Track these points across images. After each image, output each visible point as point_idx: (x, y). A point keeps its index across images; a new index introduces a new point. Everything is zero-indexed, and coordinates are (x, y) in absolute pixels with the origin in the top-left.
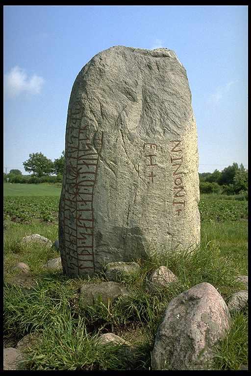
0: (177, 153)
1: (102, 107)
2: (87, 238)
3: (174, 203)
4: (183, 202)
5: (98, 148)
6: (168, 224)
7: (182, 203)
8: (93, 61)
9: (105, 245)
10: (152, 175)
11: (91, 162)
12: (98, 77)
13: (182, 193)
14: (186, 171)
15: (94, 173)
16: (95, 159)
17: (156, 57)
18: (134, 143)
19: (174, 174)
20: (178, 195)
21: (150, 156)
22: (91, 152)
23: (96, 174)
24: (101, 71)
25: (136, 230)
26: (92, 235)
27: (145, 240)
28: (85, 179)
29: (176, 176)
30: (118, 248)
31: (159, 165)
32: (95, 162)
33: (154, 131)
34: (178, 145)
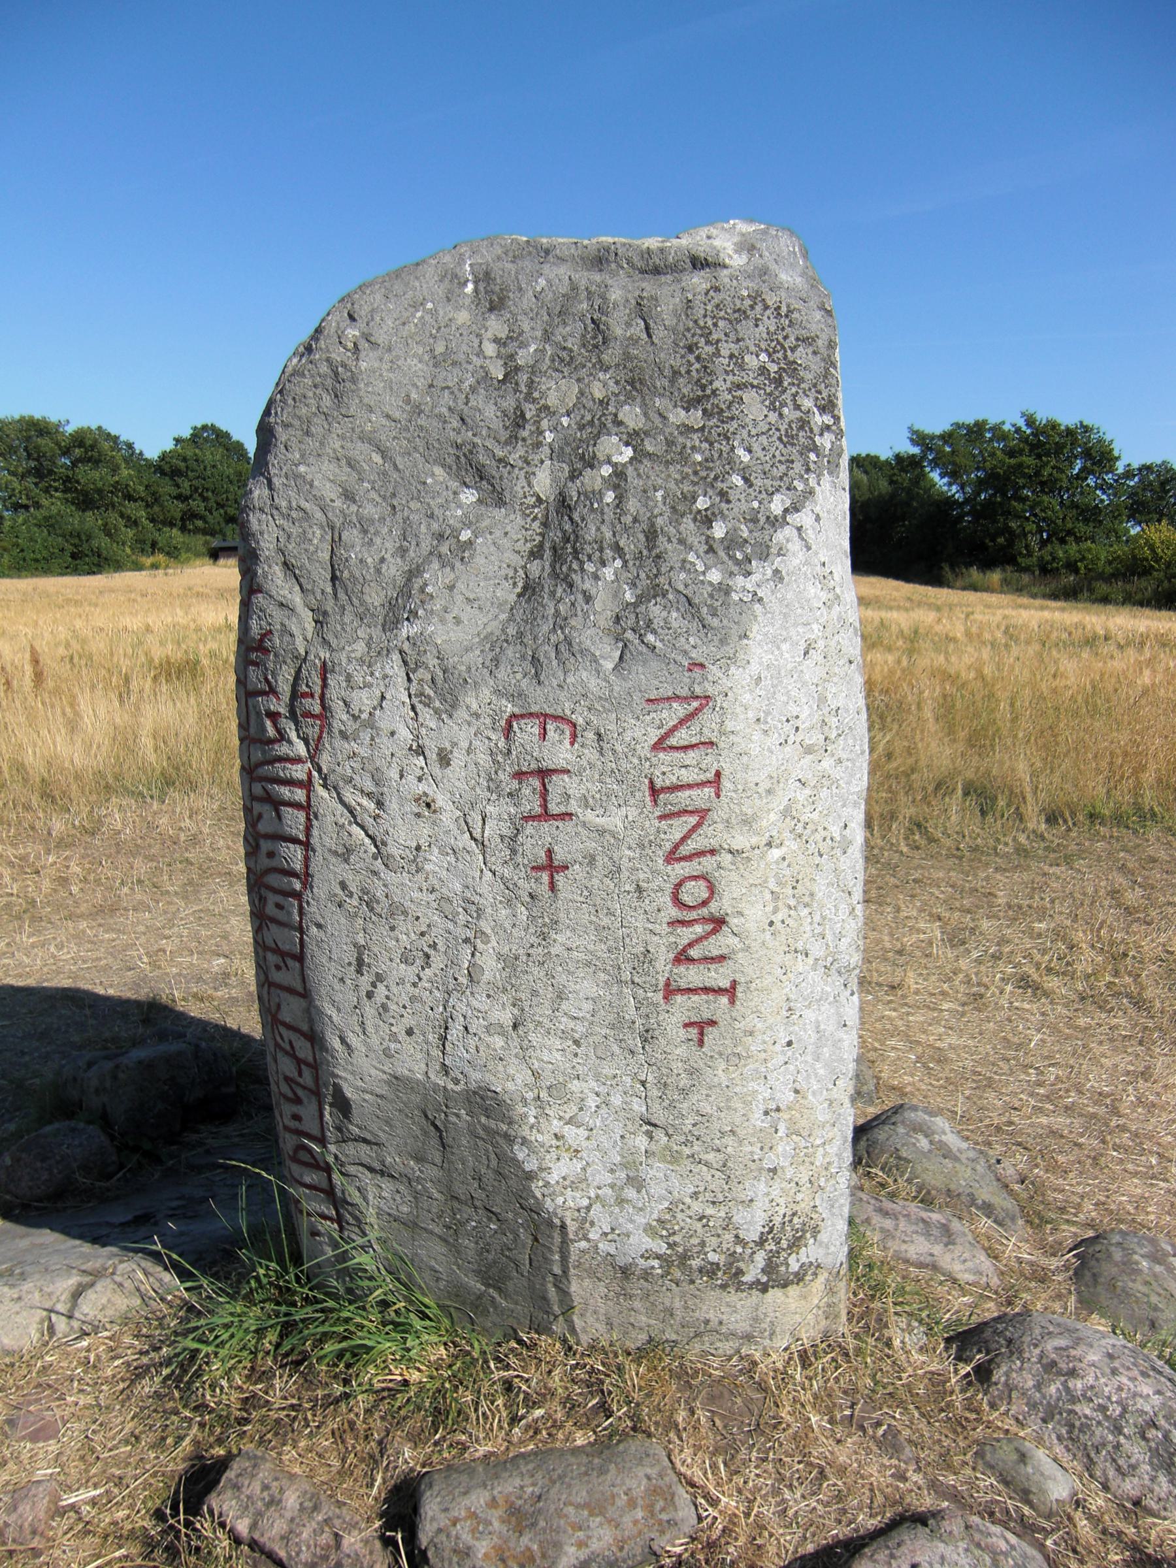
0: (691, 757)
2: (305, 1100)
3: (670, 991)
4: (725, 984)
5: (309, 731)
6: (643, 1083)
7: (719, 991)
8: (319, 331)
9: (365, 1141)
10: (551, 866)
11: (285, 792)
12: (327, 401)
13: (714, 946)
14: (740, 841)
15: (295, 841)
16: (299, 784)
17: (657, 271)
20: (694, 953)
21: (544, 774)
22: (283, 749)
23: (307, 845)
24: (336, 374)
25: (486, 1103)
26: (317, 1094)
28: (273, 863)
29: (681, 869)
30: (419, 1159)
31: (590, 816)
32: (300, 795)
33: (567, 650)
34: (698, 710)
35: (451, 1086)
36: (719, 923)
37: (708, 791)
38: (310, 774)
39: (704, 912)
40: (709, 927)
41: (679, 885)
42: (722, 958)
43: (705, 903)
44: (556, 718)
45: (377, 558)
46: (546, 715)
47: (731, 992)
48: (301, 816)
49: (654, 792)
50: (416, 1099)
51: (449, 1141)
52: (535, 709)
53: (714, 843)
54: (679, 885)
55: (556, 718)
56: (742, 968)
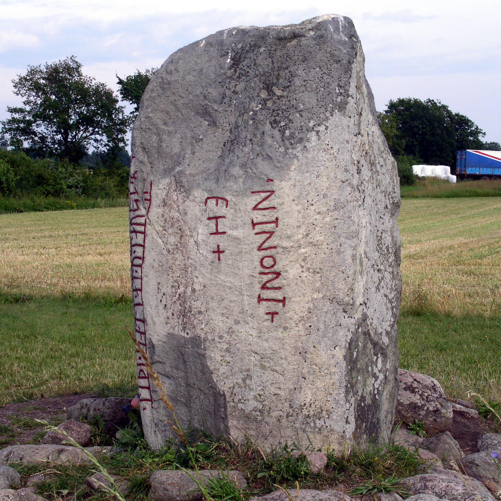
0: (266, 212)
1: (161, 140)
3: (260, 299)
4: (281, 298)
10: (218, 251)
12: (161, 91)
13: (276, 283)
14: (286, 243)
18: (191, 197)
19: (260, 249)
21: (216, 218)
23: (143, 246)
25: (196, 342)
27: (211, 358)
30: (177, 369)
32: (142, 229)
35: (186, 336)
36: (278, 274)
37: (273, 225)
38: (146, 221)
39: (272, 270)
40: (275, 276)
41: (262, 259)
42: (279, 288)
43: (272, 266)
44: (221, 198)
45: (173, 144)
46: (219, 198)
47: (283, 301)
48: (142, 236)
49: (254, 225)
50: (175, 342)
51: (186, 359)
52: (215, 195)
53: (275, 243)
54: (262, 259)
55: (221, 198)
56: (288, 292)
